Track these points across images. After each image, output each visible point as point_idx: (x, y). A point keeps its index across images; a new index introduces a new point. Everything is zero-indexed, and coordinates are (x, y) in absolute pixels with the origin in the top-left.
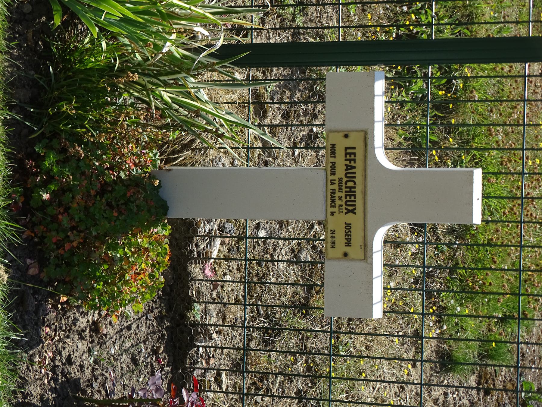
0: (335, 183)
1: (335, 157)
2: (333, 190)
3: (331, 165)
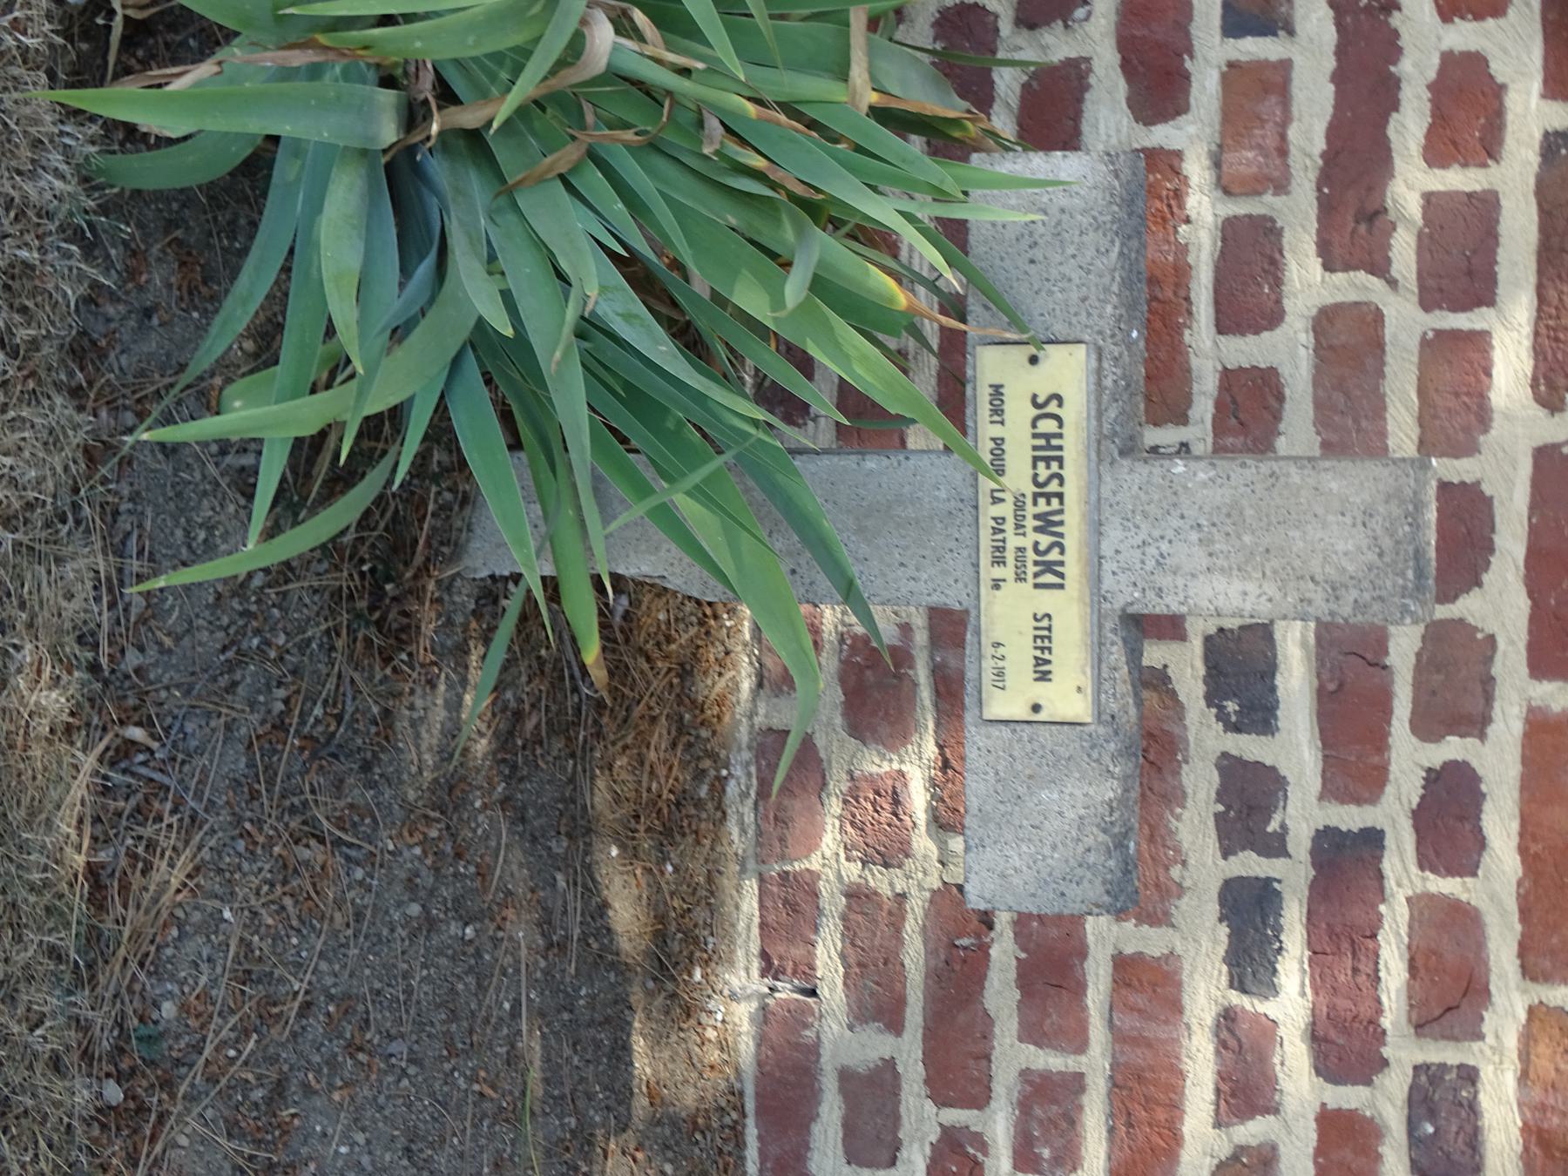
0: (1002, 500)
1: (1002, 423)
2: (994, 519)
3: (992, 445)
